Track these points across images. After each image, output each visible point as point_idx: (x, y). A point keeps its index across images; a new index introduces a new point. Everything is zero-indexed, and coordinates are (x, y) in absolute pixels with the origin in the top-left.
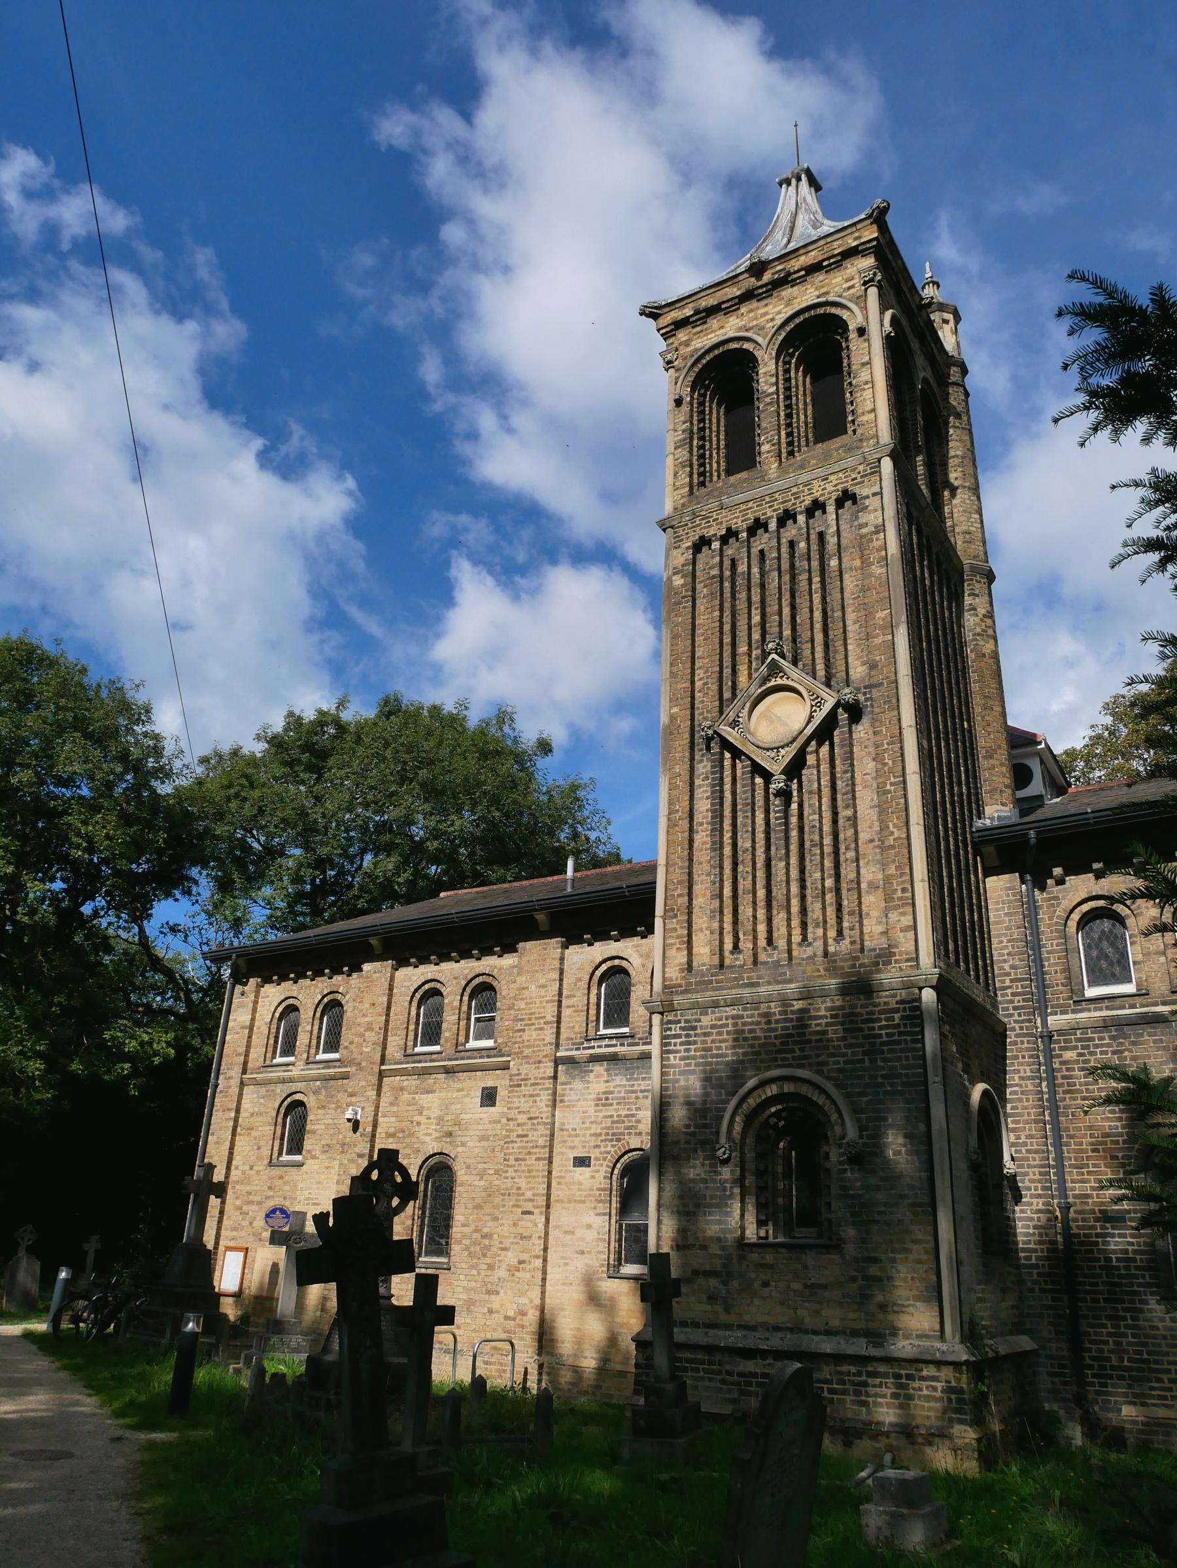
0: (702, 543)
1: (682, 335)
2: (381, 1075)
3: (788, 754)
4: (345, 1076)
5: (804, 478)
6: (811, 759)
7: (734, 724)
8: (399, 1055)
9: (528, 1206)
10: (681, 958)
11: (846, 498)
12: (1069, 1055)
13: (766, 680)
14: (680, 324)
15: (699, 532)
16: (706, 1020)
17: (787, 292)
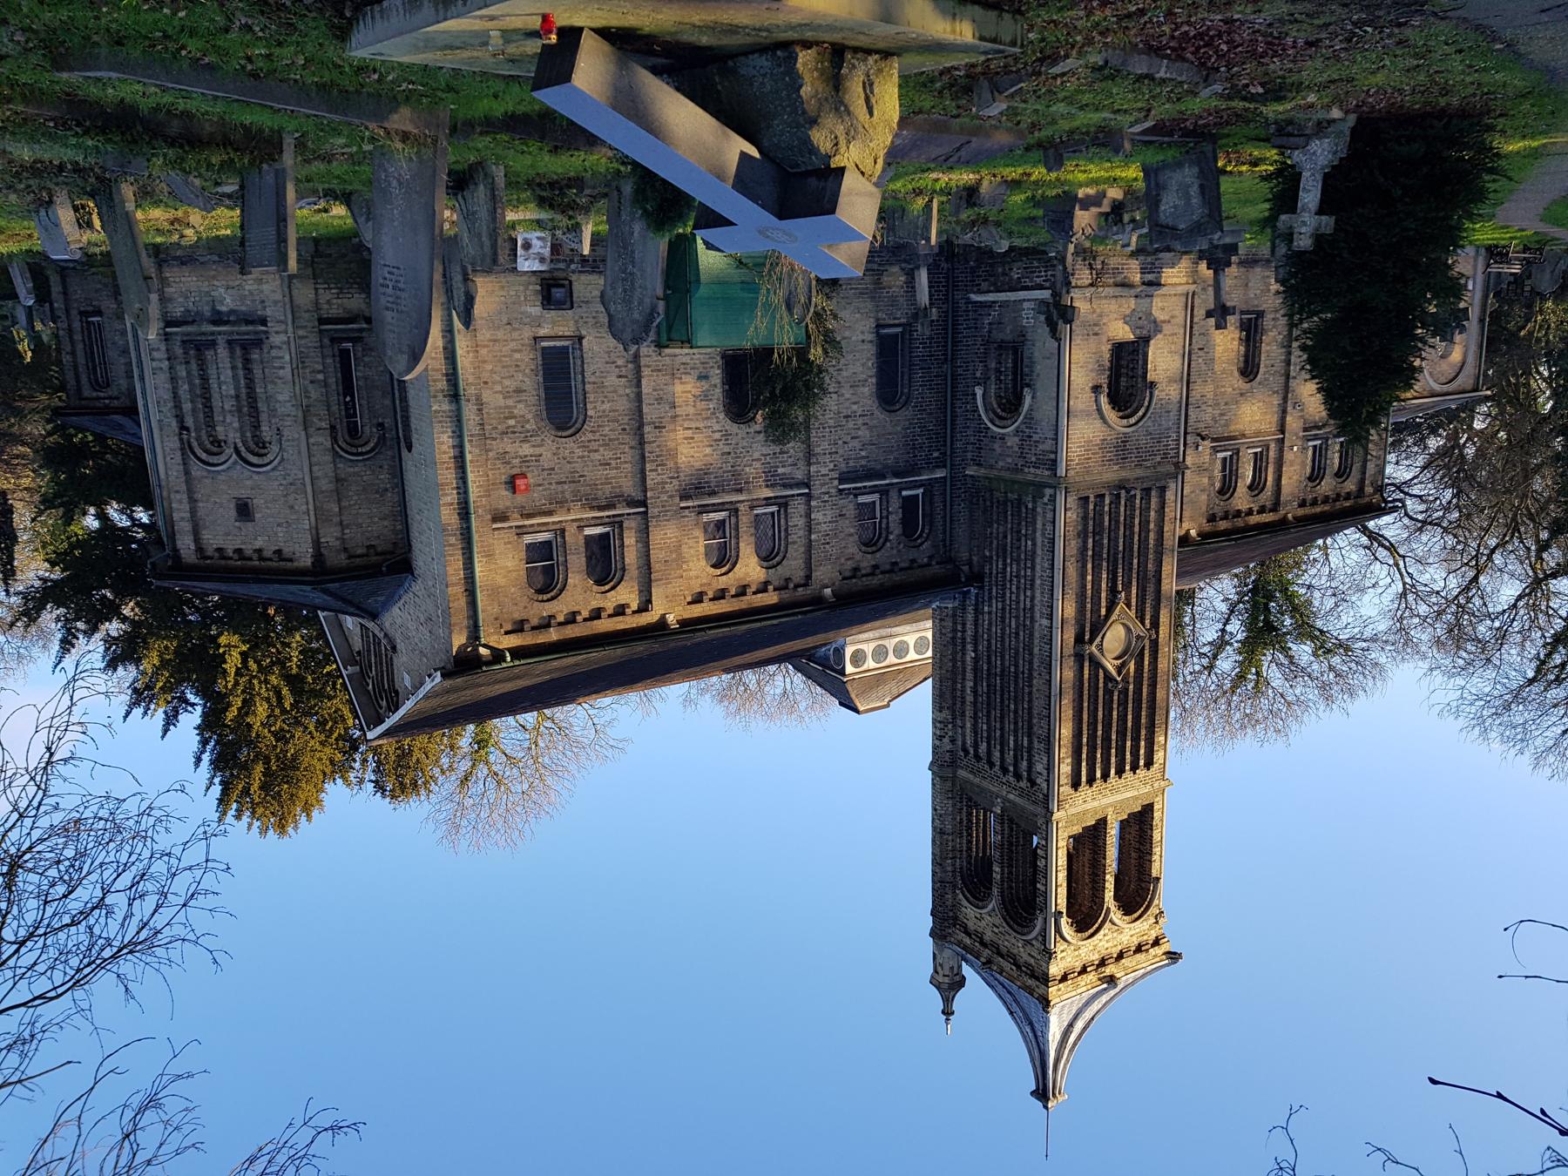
0: (1149, 764)
1: (1153, 934)
2: (1283, 432)
3: (1113, 618)
4: (1305, 430)
5: (1096, 804)
6: (1103, 612)
7: (1138, 637)
8: (1273, 445)
9: (1201, 353)
10: (1170, 495)
11: (1076, 785)
12: (936, 454)
13: (1123, 665)
14: (1156, 943)
15: (1150, 773)
16: (1158, 459)
17: (1096, 957)
